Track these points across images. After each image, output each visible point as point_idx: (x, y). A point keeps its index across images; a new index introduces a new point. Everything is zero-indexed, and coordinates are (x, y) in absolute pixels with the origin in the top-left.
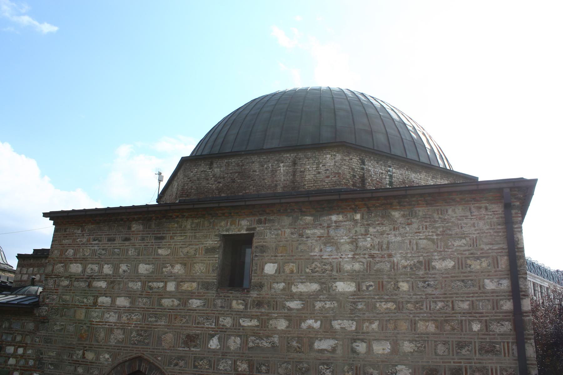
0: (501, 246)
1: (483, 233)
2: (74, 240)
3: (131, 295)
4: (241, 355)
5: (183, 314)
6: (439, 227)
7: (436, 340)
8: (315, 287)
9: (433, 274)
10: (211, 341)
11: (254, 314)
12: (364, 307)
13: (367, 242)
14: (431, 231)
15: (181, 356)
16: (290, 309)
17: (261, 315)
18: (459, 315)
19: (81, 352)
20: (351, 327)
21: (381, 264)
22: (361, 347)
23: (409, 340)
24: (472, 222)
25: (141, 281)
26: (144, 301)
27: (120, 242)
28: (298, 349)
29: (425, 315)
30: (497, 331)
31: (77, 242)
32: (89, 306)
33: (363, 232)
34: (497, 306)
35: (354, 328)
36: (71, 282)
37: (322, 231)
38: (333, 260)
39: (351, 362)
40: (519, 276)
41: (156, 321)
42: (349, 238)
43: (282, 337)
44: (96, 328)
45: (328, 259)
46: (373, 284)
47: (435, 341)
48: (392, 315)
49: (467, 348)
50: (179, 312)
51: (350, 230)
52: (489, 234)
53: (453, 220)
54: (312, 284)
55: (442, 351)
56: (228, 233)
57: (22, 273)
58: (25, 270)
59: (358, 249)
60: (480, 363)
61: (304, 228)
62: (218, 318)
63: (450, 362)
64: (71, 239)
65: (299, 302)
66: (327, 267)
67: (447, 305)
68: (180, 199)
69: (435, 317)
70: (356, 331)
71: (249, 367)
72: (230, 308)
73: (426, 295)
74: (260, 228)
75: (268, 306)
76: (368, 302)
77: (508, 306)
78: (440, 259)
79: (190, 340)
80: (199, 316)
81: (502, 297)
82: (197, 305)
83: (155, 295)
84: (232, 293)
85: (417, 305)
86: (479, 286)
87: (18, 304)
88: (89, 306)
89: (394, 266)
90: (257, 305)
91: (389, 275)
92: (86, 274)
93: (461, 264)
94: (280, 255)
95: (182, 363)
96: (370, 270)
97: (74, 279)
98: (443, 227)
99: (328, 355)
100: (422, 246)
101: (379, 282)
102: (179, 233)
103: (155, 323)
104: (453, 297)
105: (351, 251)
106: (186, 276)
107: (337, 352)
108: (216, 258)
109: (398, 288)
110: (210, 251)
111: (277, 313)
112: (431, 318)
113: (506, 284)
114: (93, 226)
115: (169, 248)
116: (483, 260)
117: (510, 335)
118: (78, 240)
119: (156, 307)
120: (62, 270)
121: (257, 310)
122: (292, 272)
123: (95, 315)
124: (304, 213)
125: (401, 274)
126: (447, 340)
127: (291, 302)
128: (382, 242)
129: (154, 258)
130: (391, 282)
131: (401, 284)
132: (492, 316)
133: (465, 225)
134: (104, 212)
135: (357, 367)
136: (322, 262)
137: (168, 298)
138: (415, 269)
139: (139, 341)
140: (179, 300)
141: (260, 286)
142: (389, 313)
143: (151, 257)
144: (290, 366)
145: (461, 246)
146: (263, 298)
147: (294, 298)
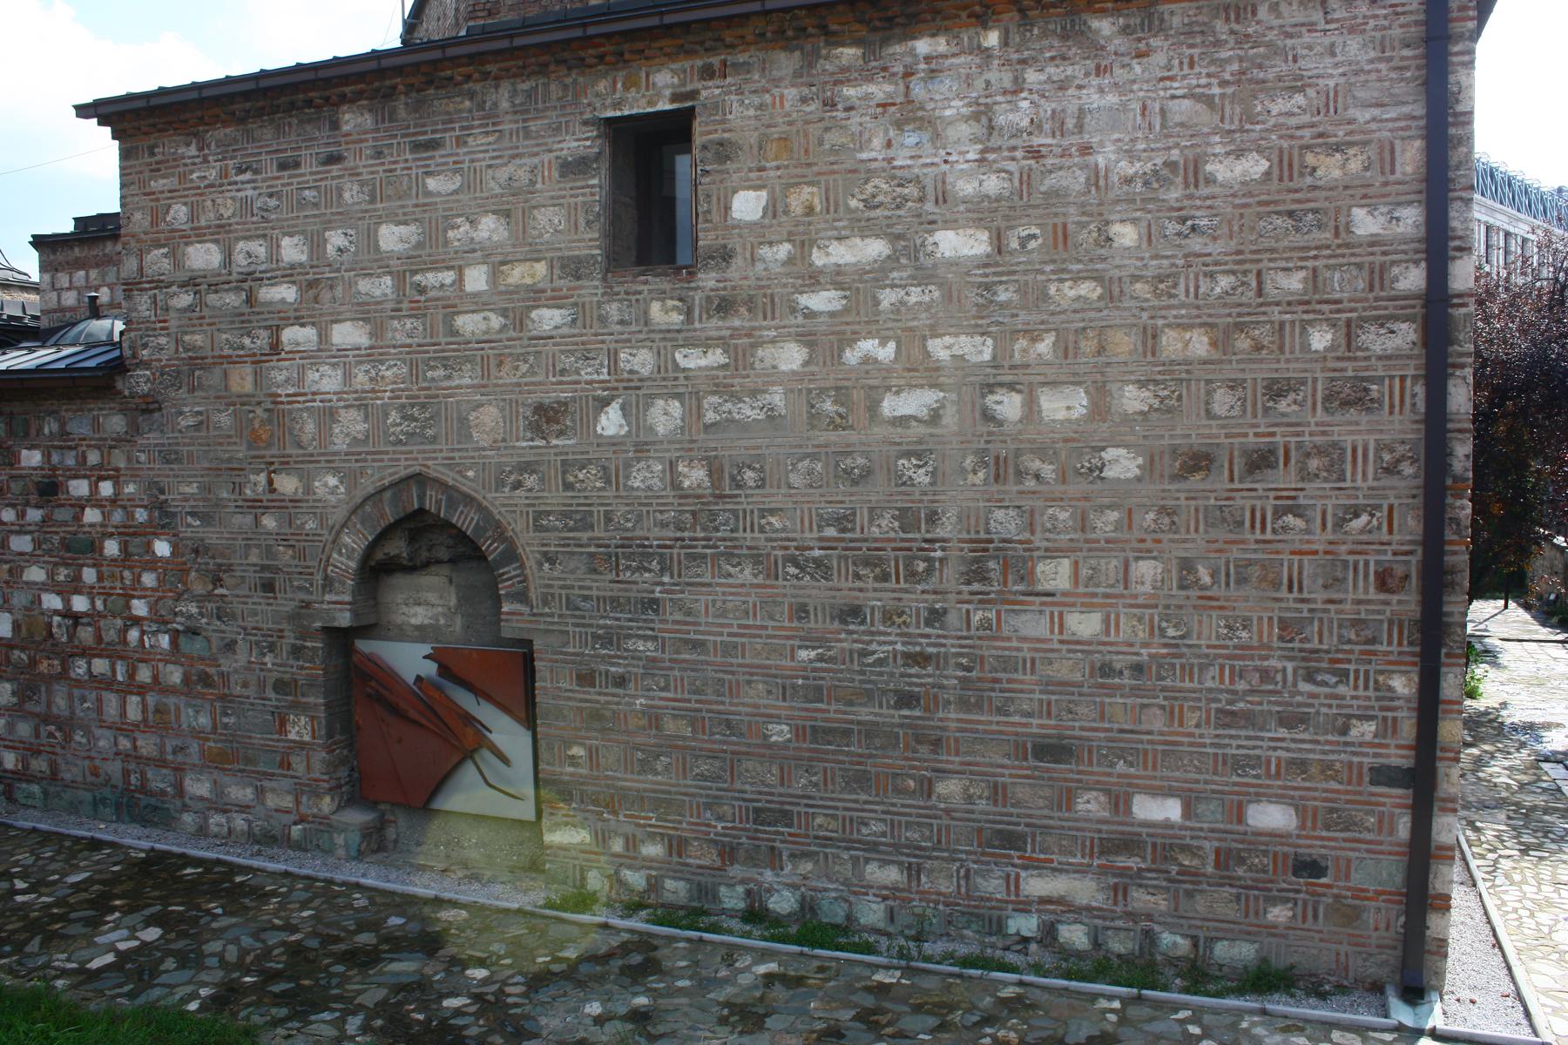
0: (1406, 109)
1: (1356, 73)
2: (183, 177)
3: (366, 312)
4: (687, 446)
5: (520, 351)
6: (1228, 61)
7: (1209, 377)
8: (876, 248)
9: (1207, 198)
10: (603, 418)
11: (714, 333)
12: (1015, 297)
13: (1016, 114)
14: (1204, 71)
15: (528, 463)
16: (810, 314)
17: (732, 336)
18: (1277, 309)
19: (262, 478)
20: (981, 352)
21: (1061, 173)
22: (1009, 406)
23: (1139, 381)
24: (1327, 41)
25: (390, 273)
26: (409, 326)
28: (838, 420)
29: (1183, 312)
30: (1377, 348)
31: (192, 181)
33: (1008, 84)
34: (1382, 278)
35: (987, 356)
37: (889, 88)
38: (925, 171)
39: (982, 445)
40: (1451, 195)
41: (449, 377)
42: (969, 105)
43: (792, 391)
44: (290, 412)
45: (909, 167)
46: (1038, 232)
47: (1208, 382)
48: (1093, 314)
49: (1292, 396)
50: (506, 347)
51: (968, 81)
52: (1374, 76)
53: (1271, 36)
54: (867, 241)
55: (1227, 407)
56: (618, 114)
57: (58, 286)
58: (63, 279)
59: (995, 133)
60: (1324, 433)
61: (836, 83)
62: (616, 353)
63: (1246, 435)
64: (173, 175)
65: (833, 294)
66: (906, 191)
67: (1243, 284)
68: (471, 23)
69: (1210, 316)
70: (995, 363)
71: (710, 474)
72: (646, 324)
73: (1186, 256)
74: (710, 91)
75: (750, 310)
76: (1026, 283)
77: (1413, 279)
78: (1228, 154)
79: (547, 417)
80: (562, 352)
81: (1395, 257)
82: (553, 323)
83: (436, 307)
84: (646, 283)
85: (1161, 286)
86: (1337, 228)
87: (67, 369)
89: (1096, 179)
90: (719, 309)
91: (1083, 205)
92: (236, 269)
93: (1286, 166)
94: (774, 164)
95: (531, 481)
96: (1029, 194)
97: (205, 287)
98: (1241, 60)
99: (917, 430)
100: (1177, 118)
101: (1055, 225)
102: (481, 126)
103: (446, 384)
104: (1260, 261)
105: (975, 140)
106: (514, 246)
107: (944, 421)
108: (593, 186)
109: (1109, 239)
110: (573, 168)
111: (776, 328)
112: (1198, 321)
113: (1411, 218)
114: (228, 130)
115: (456, 171)
116: (1351, 152)
117: (1409, 357)
118: (194, 176)
119: (443, 340)
120: (166, 264)
121: (720, 323)
122: (810, 210)
123: (280, 377)
124: (834, 39)
125: (1117, 202)
126: (1240, 376)
127: (813, 296)
128: (1063, 111)
129: (417, 206)
130: (1088, 223)
131: (1116, 228)
132: (1365, 309)
133: (1305, 52)
134: (251, 86)
135: (997, 458)
136: (893, 177)
137: (473, 312)
138: (1155, 185)
139: (411, 435)
140: (504, 313)
141: (725, 256)
142: (1083, 310)
143: (410, 203)
144: (819, 467)
145: (1290, 114)
146: (734, 288)
147: (818, 283)
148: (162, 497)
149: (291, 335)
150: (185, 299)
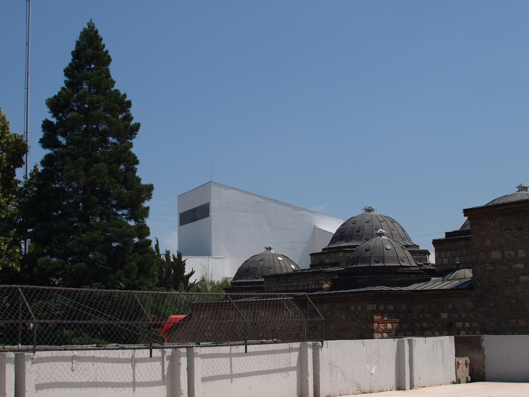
19: (514, 321)
27: (527, 230)
31: (492, 233)
32: (514, 284)
36: (494, 267)
58: (443, 255)
88: (514, 284)
114: (502, 218)
118: (492, 231)
148: (484, 327)
149: (522, 278)
150: (491, 268)
